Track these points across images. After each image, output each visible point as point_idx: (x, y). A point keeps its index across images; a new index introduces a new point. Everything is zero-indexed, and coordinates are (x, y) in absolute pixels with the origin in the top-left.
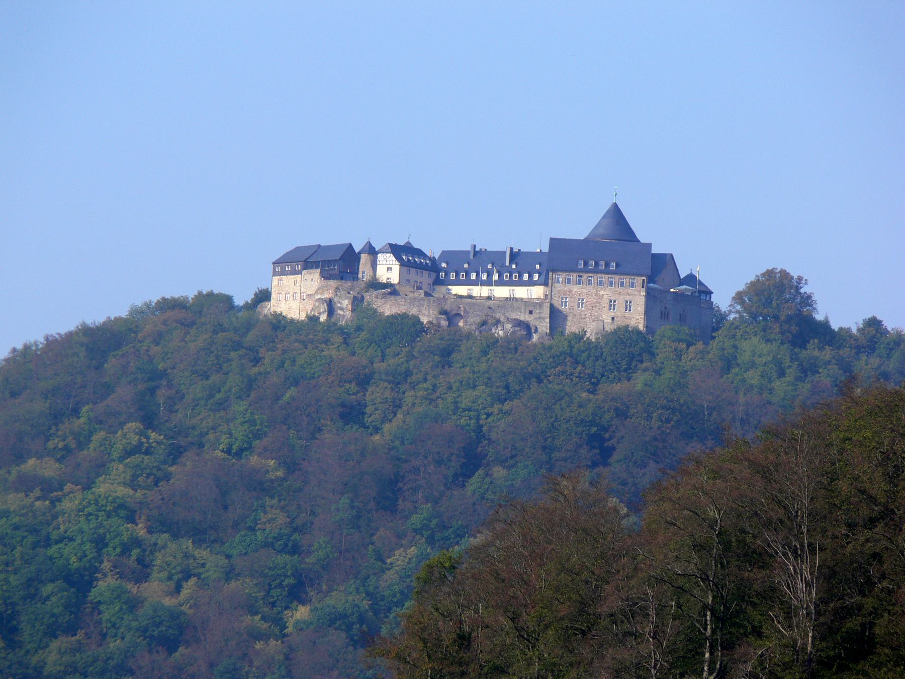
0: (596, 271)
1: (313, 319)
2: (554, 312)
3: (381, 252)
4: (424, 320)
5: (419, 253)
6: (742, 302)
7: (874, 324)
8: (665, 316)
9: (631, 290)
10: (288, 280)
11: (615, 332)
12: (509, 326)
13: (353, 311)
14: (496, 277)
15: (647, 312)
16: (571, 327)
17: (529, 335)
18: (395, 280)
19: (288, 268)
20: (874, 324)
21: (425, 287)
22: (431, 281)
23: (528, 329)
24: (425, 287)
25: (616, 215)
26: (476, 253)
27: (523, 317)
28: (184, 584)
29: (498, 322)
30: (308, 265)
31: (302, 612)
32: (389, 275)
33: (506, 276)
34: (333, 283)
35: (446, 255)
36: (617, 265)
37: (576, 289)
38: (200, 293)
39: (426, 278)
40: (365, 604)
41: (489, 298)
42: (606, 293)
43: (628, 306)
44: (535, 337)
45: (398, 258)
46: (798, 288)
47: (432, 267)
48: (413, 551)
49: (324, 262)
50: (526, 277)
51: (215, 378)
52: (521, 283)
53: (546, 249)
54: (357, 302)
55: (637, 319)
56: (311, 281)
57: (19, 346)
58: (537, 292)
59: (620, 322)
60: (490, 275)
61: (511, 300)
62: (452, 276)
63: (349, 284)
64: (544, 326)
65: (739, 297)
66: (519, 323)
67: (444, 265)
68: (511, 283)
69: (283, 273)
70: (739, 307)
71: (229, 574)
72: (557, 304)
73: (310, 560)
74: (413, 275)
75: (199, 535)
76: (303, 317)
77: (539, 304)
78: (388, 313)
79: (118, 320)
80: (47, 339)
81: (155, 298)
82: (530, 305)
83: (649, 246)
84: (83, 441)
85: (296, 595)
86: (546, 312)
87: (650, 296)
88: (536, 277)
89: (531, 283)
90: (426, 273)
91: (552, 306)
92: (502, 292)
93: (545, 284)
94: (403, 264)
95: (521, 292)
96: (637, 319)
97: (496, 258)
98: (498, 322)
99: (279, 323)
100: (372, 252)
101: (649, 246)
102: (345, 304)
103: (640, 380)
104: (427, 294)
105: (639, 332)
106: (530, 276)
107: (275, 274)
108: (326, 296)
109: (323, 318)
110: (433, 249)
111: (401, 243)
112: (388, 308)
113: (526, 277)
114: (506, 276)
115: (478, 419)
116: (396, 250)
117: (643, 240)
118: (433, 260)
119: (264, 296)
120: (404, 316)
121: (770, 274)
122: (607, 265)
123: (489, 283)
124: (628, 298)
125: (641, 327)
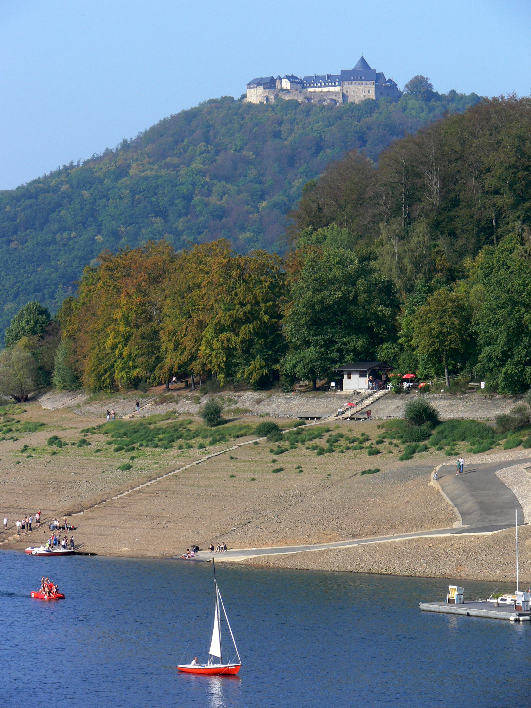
0: (357, 80)
1: (261, 103)
2: (344, 95)
3: (283, 78)
4: (300, 101)
5: (296, 78)
6: (408, 88)
7: (453, 92)
8: (382, 94)
9: (369, 86)
10: (252, 90)
11: (365, 101)
12: (329, 101)
13: (275, 99)
14: (323, 84)
15: (376, 93)
16: (350, 100)
17: (336, 103)
18: (289, 88)
19: (252, 86)
20: (453, 92)
21: (299, 90)
22: (301, 87)
23: (335, 101)
24: (299, 90)
25: (363, 60)
26: (316, 77)
27: (334, 97)
28: (224, 197)
29: (325, 100)
30: (259, 85)
31: (264, 204)
32: (286, 86)
33: (327, 84)
34: (267, 90)
35: (305, 78)
36: (364, 78)
37: (351, 87)
38: (222, 97)
39: (299, 86)
40: (286, 199)
41: (321, 92)
42: (361, 88)
43: (369, 91)
44: (338, 104)
45: (289, 80)
46: (426, 82)
47: (301, 82)
48: (301, 180)
49: (264, 83)
50: (333, 84)
51: (229, 126)
52: (332, 86)
53: (340, 74)
54: (276, 96)
55: (372, 95)
56: (260, 90)
57: (162, 119)
58: (337, 89)
59: (366, 97)
60: (321, 84)
61: (329, 92)
62: (308, 85)
63: (273, 90)
64: (341, 100)
65: (407, 86)
66: (332, 100)
67: (305, 82)
68: (329, 86)
69: (250, 88)
70: (407, 89)
71: (239, 192)
72: (345, 92)
73: (266, 186)
74: (295, 85)
75: (228, 179)
76: (258, 103)
77: (338, 93)
78: (287, 99)
79: (195, 108)
80: (171, 116)
81: (207, 99)
82: (335, 93)
83: (375, 70)
84: (186, 150)
85: (262, 197)
86: (341, 95)
87: (377, 88)
88: (337, 83)
89: (335, 86)
90: (299, 85)
91: (343, 93)
92: (325, 89)
93: (340, 86)
94: (291, 82)
95: (332, 89)
96: (372, 95)
97: (323, 78)
98: (325, 100)
99: (250, 105)
100: (280, 79)
101: (375, 70)
102: (272, 97)
103: (375, 116)
104: (300, 92)
105: (372, 100)
106: (335, 83)
107: (248, 88)
108: (266, 95)
109: (265, 102)
110: (301, 77)
111: (290, 75)
112: (287, 98)
113: (333, 84)
114: (327, 84)
115: (320, 133)
116: (288, 78)
117: (373, 69)
118: (301, 80)
119: (244, 96)
120: (293, 100)
121: (417, 77)
122: (361, 78)
123: (321, 86)
124: (369, 89)
125: (374, 98)
